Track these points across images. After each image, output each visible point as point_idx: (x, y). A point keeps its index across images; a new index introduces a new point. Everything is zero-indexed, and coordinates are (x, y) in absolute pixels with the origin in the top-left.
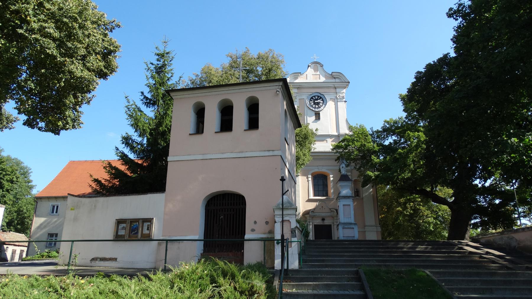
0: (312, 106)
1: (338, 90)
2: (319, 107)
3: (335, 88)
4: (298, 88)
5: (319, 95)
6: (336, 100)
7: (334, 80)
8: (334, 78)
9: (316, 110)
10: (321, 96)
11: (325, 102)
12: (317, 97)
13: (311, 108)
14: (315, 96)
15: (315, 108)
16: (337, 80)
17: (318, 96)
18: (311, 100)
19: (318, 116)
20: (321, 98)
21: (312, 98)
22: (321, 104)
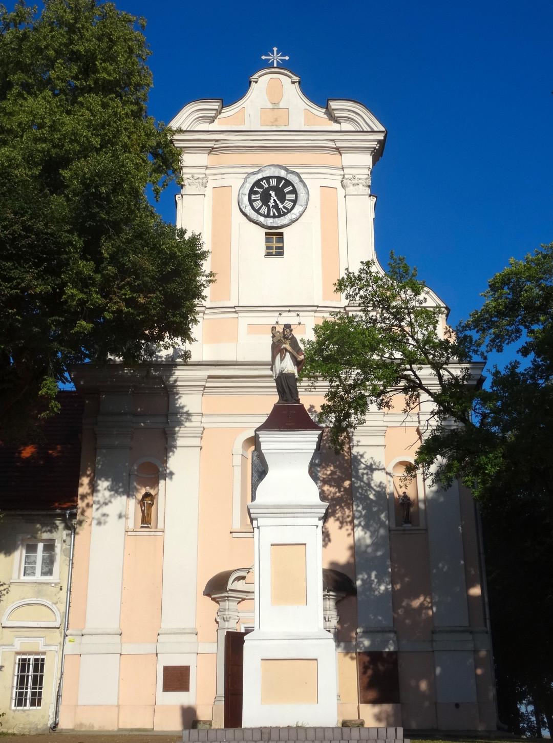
0: (257, 211)
1: (348, 159)
2: (280, 216)
3: (338, 150)
4: (212, 150)
5: (283, 173)
6: (341, 192)
7: (336, 127)
8: (336, 120)
9: (270, 222)
10: (291, 177)
11: (302, 195)
12: (273, 182)
13: (254, 215)
14: (267, 179)
15: (268, 216)
16: (346, 126)
17: (279, 179)
18: (252, 192)
19: (275, 244)
20: (288, 183)
21: (257, 183)
22: (289, 205)
